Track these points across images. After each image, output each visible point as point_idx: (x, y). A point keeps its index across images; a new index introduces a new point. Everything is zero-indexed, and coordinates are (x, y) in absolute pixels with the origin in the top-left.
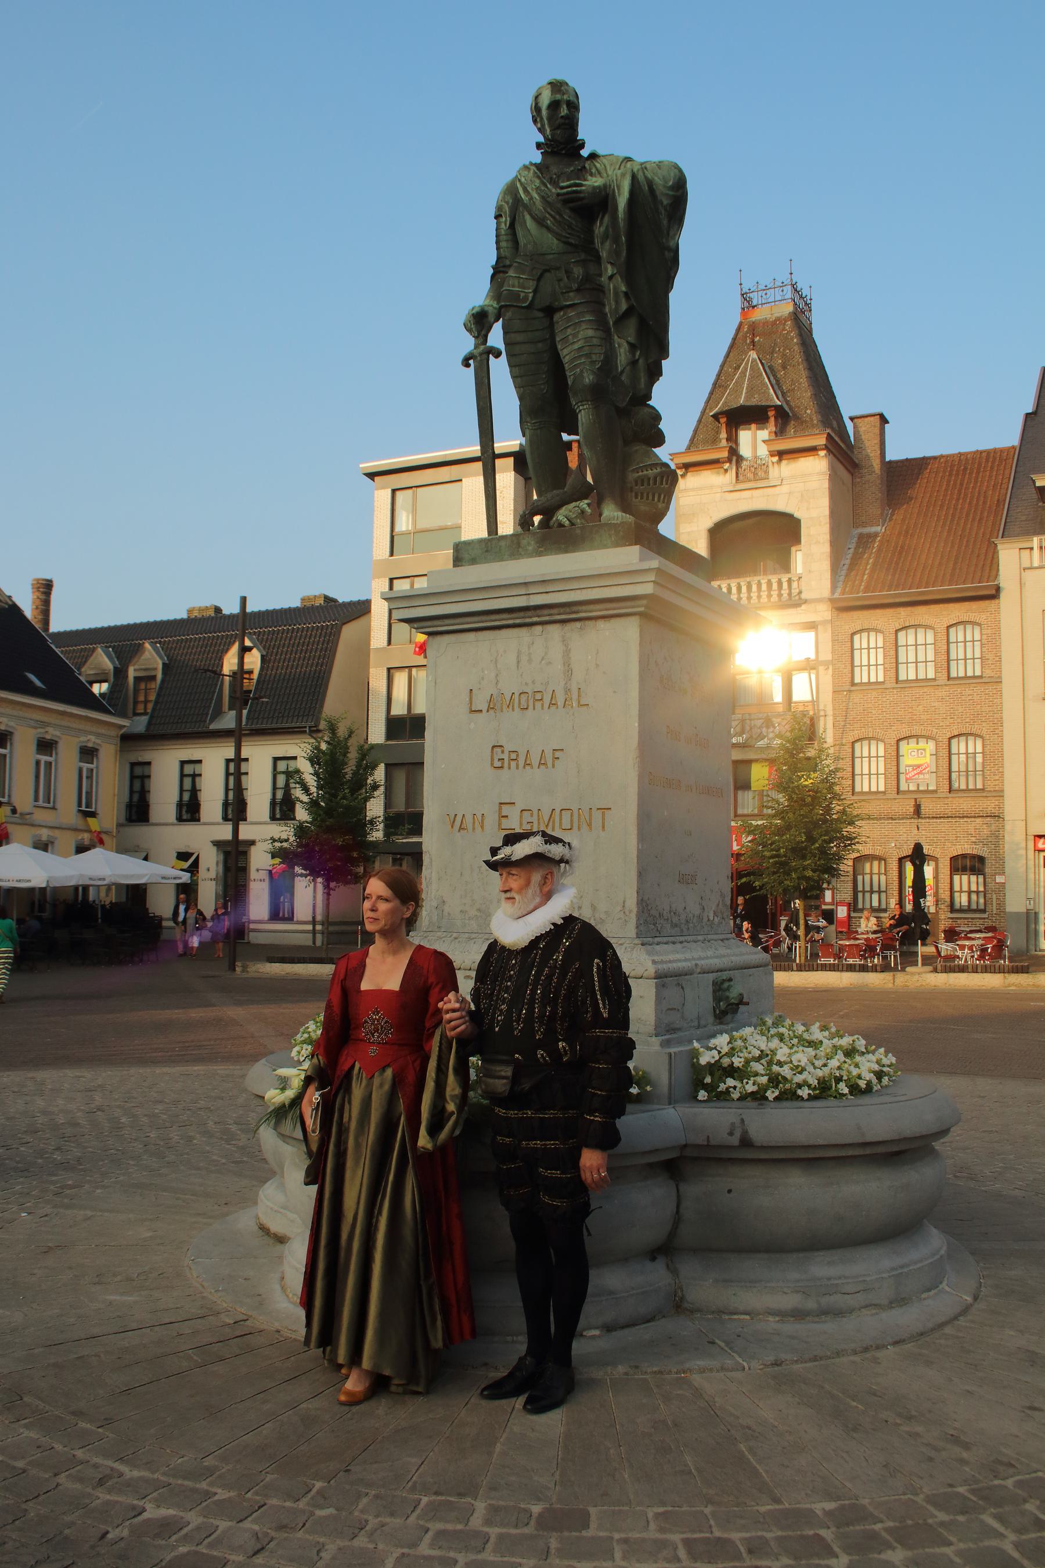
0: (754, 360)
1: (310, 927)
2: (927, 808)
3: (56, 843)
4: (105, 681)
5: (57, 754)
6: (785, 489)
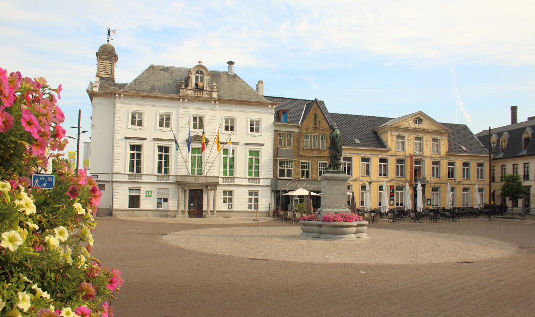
3: (470, 188)
4: (495, 143)
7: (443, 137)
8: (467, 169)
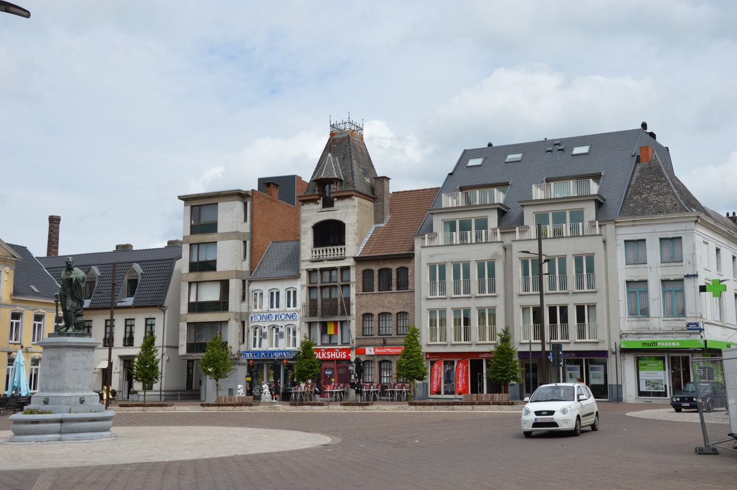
0: (330, 157)
1: (159, 393)
2: (389, 341)
5: (44, 321)
6: (340, 211)
7: (8, 269)
8: (17, 324)
